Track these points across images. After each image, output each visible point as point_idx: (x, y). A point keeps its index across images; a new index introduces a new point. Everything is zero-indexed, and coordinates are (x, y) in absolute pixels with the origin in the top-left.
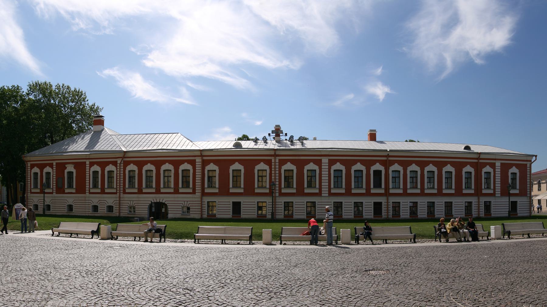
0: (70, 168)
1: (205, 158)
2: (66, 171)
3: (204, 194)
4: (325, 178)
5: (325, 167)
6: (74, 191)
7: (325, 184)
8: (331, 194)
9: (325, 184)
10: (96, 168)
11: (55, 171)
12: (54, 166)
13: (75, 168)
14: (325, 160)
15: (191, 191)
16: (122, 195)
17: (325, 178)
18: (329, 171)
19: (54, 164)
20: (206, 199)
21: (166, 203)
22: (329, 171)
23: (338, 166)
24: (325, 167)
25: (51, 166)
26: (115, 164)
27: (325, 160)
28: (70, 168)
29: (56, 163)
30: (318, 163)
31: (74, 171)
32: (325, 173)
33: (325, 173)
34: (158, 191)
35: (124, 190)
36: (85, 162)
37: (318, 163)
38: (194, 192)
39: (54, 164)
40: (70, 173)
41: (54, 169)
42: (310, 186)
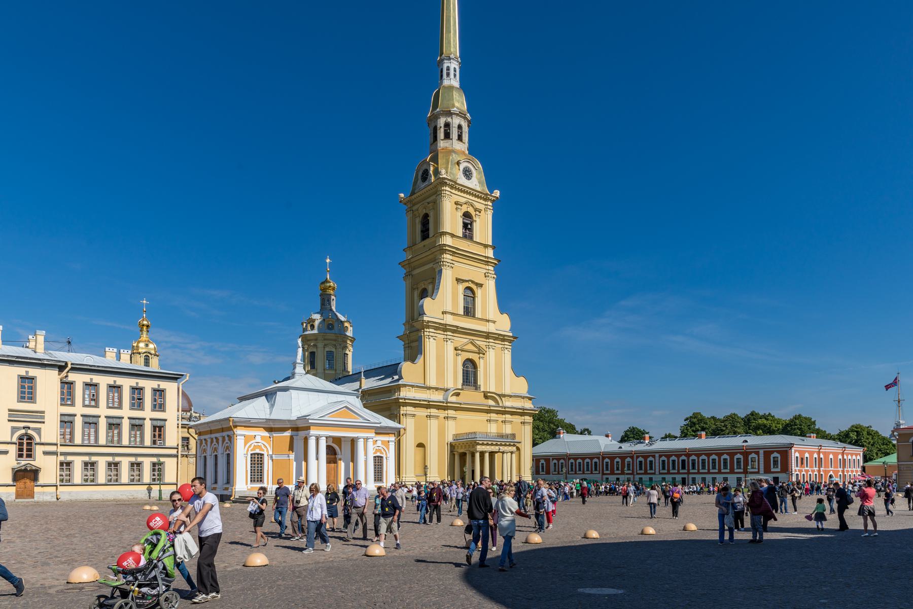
0: (542, 461)
2: (540, 463)
3: (603, 474)
4: (657, 465)
5: (657, 458)
6: (545, 473)
7: (657, 468)
8: (660, 474)
9: (657, 468)
14: (657, 455)
16: (568, 475)
17: (657, 465)
23: (663, 458)
24: (657, 458)
27: (657, 455)
28: (542, 461)
30: (654, 457)
31: (545, 463)
34: (584, 473)
36: (550, 459)
37: (654, 457)
38: (599, 473)
40: (542, 464)
42: (651, 468)
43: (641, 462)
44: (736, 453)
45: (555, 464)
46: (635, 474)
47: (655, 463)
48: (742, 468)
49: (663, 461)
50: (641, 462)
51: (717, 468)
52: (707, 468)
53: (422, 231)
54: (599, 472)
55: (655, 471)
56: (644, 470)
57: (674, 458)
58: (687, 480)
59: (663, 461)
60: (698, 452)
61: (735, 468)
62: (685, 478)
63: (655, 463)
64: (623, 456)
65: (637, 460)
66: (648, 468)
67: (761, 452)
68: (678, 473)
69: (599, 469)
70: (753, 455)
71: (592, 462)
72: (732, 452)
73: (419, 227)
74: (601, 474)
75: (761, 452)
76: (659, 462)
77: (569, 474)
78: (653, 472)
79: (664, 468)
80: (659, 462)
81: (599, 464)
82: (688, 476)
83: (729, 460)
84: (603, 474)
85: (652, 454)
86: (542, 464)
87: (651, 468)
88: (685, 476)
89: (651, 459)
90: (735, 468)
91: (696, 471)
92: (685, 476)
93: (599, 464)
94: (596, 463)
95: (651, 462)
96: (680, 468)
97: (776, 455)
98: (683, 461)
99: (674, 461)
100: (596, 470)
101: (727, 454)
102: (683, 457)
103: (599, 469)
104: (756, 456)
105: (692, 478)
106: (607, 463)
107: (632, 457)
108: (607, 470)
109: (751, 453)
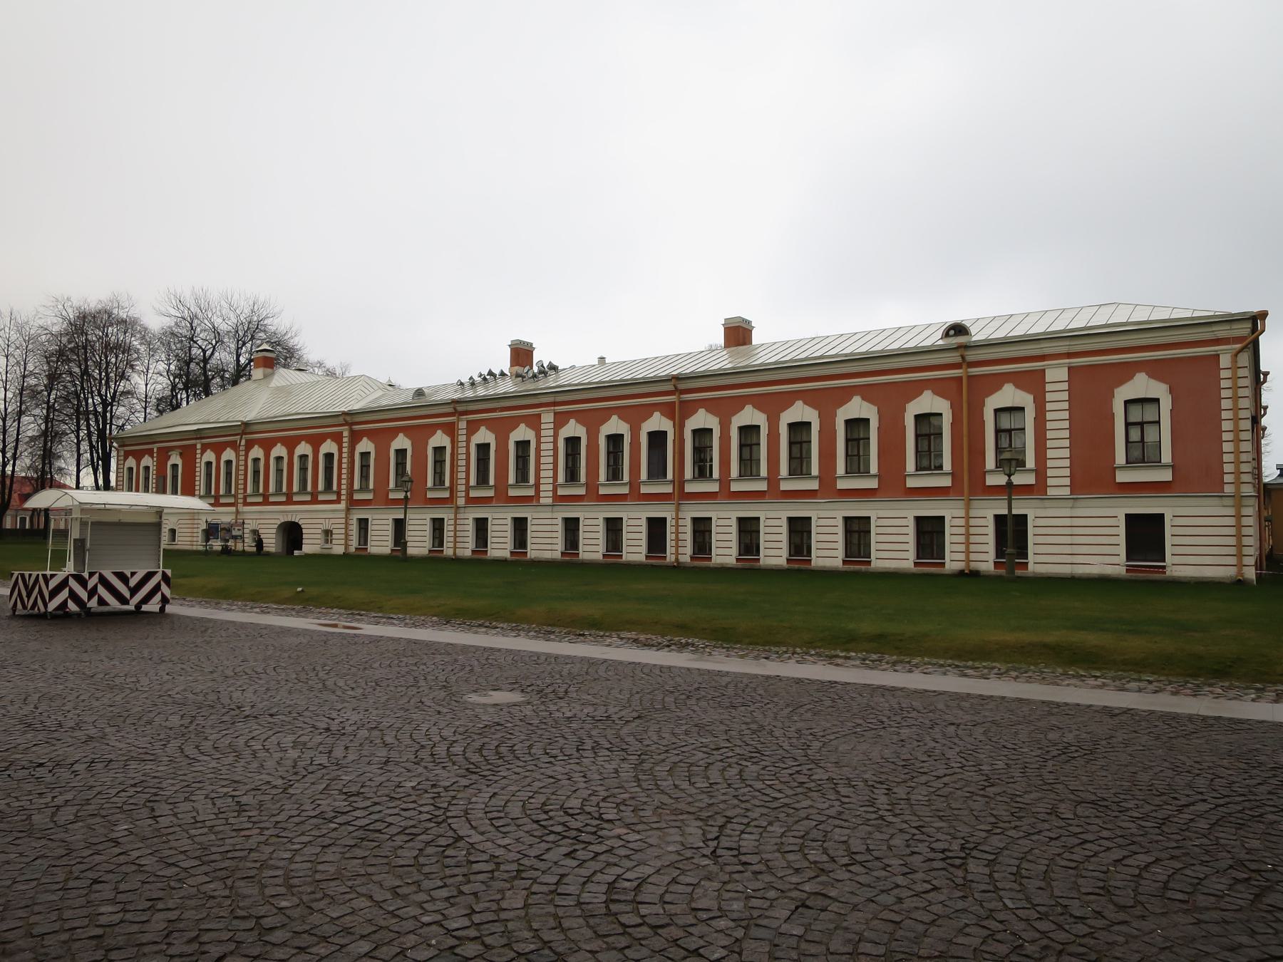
0: (175, 459)
1: (356, 427)
2: (169, 463)
3: (353, 504)
4: (547, 460)
5: (547, 432)
7: (546, 474)
8: (559, 499)
9: (546, 474)
10: (210, 456)
11: (155, 463)
12: (155, 455)
13: (181, 454)
14: (547, 418)
15: (334, 497)
17: (547, 460)
18: (555, 443)
19: (155, 450)
20: (357, 515)
21: (300, 523)
22: (555, 443)
24: (547, 432)
25: (150, 452)
26: (234, 446)
27: (547, 418)
28: (175, 459)
29: (158, 449)
30: (534, 423)
32: (547, 446)
33: (547, 446)
34: (289, 501)
35: (245, 498)
36: (195, 445)
37: (534, 423)
38: (338, 501)
39: (155, 450)
40: (175, 466)
41: (155, 459)
42: (522, 476)
43: (483, 448)
44: (915, 389)
45: (209, 464)
46: (461, 502)
47: (538, 450)
48: (947, 466)
49: (573, 442)
50: (483, 448)
51: (815, 471)
52: (764, 472)
54: (339, 494)
55: (538, 490)
57: (615, 425)
58: (670, 529)
59: (573, 442)
61: (910, 466)
62: (663, 521)
63: (538, 450)
65: (468, 441)
66: (512, 479)
67: (1057, 374)
68: (636, 496)
69: (339, 484)
70: (1009, 395)
71: (316, 452)
74: (342, 506)
75: (1057, 374)
76: (555, 449)
77: (246, 504)
78: (531, 492)
79: (572, 475)
80: (555, 449)
81: (340, 463)
82: (678, 511)
83: (874, 425)
84: (353, 504)
86: (175, 466)
87: (522, 476)
88: (664, 511)
90: (910, 466)
91: (714, 487)
92: (664, 511)
93: (340, 463)
95: (523, 446)
96: (644, 475)
97: (1141, 386)
98: (657, 439)
99: (615, 440)
101: (867, 393)
102: (657, 422)
103: (339, 484)
104: (1023, 399)
105: (696, 521)
106: (365, 455)
107: (450, 430)
108: (364, 488)
109: (995, 383)
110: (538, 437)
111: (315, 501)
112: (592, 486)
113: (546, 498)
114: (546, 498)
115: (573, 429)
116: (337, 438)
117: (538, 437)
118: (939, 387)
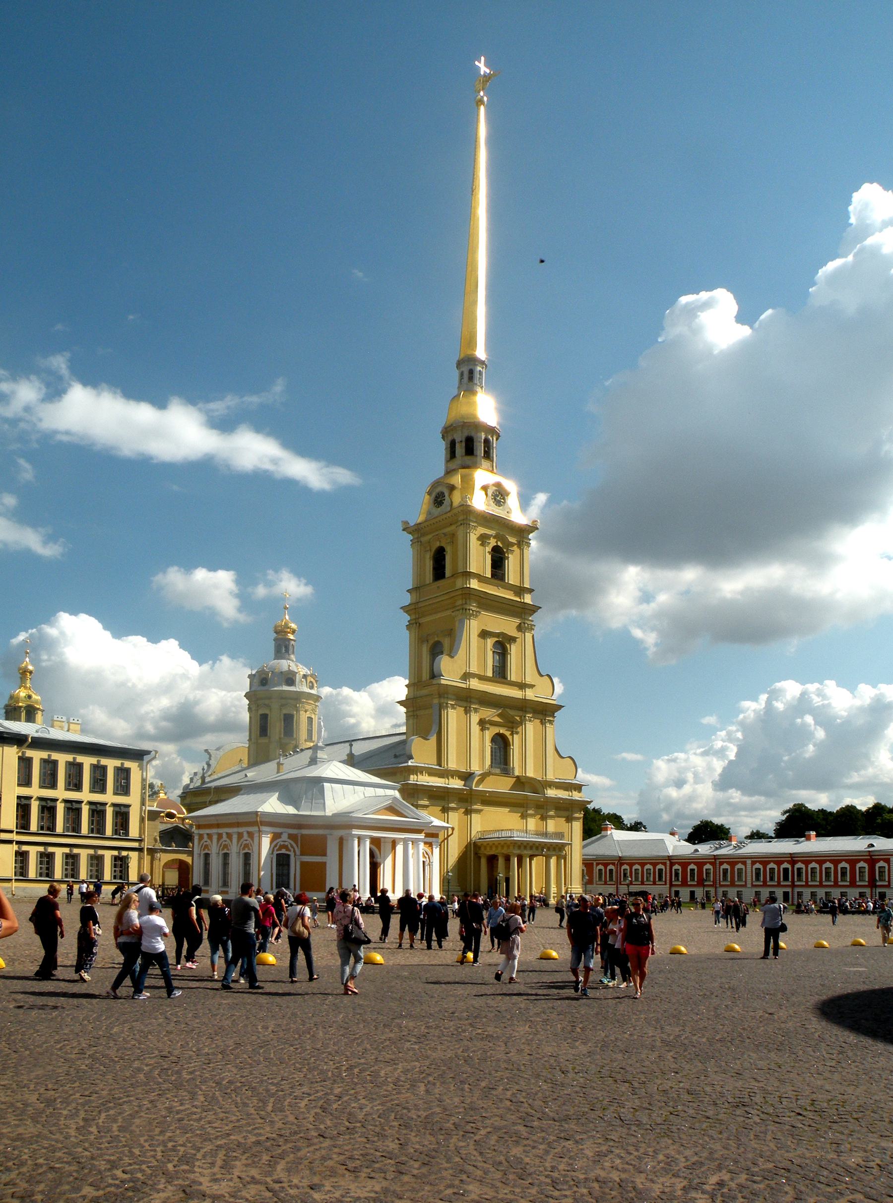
3: (671, 885)
4: (749, 874)
7: (749, 878)
8: (753, 886)
9: (749, 878)
14: (749, 862)
17: (749, 874)
20: (674, 889)
23: (758, 866)
27: (749, 862)
30: (744, 863)
32: (749, 870)
33: (749, 870)
34: (643, 883)
37: (744, 863)
38: (666, 884)
43: (725, 871)
44: (859, 861)
53: (434, 569)
54: (666, 881)
56: (731, 881)
59: (758, 870)
60: (807, 859)
61: (858, 879)
62: (788, 892)
64: (700, 862)
70: (881, 864)
72: (852, 859)
73: (429, 565)
74: (668, 886)
77: (621, 884)
79: (758, 879)
81: (666, 874)
85: (743, 859)
89: (740, 866)
93: (666, 874)
94: (660, 870)
95: (740, 870)
96: (782, 879)
99: (772, 870)
100: (660, 879)
110: (746, 867)
111: (654, 883)
112: (765, 881)
113: (749, 885)
114: (749, 885)
115: (758, 866)
116: (665, 864)
117: (746, 867)
118: (865, 861)
